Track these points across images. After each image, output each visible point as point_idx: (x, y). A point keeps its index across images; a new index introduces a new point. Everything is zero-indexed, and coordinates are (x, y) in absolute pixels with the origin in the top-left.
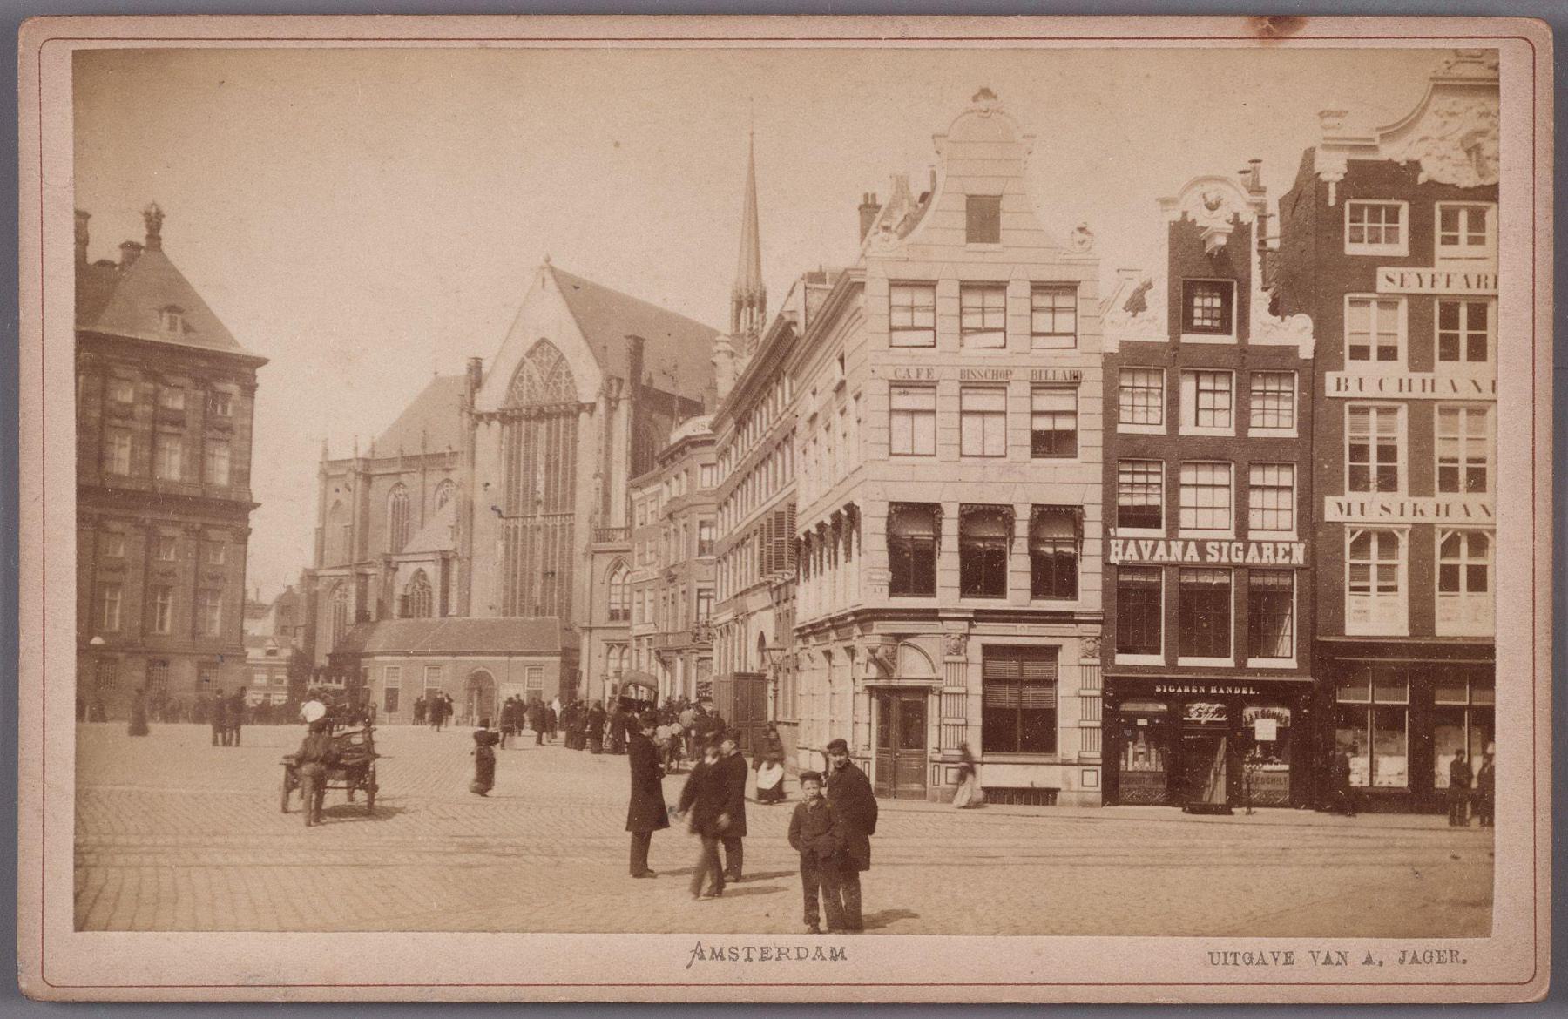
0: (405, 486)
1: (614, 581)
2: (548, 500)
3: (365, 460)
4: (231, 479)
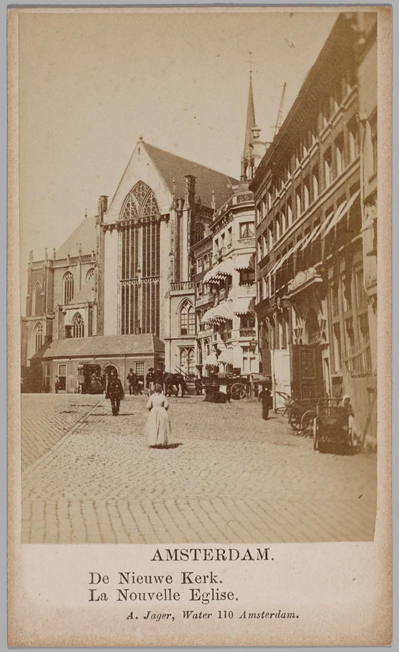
0: (71, 274)
1: (183, 312)
2: (144, 270)
3: (52, 261)
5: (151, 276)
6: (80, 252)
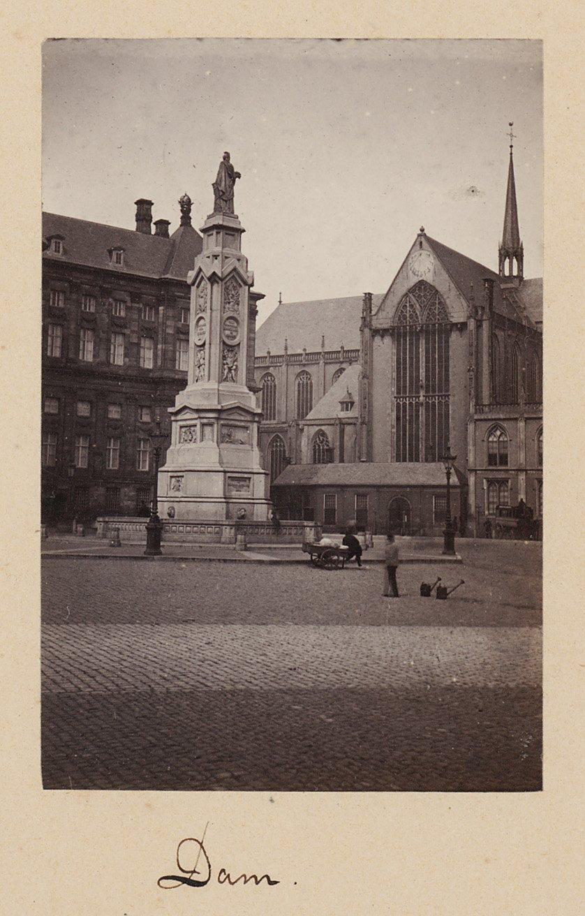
0: (271, 375)
1: (490, 439)
2: (427, 386)
5: (437, 394)
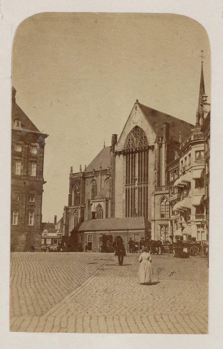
0: (95, 181)
1: (162, 204)
2: (139, 179)
4: (37, 174)
6: (101, 167)
